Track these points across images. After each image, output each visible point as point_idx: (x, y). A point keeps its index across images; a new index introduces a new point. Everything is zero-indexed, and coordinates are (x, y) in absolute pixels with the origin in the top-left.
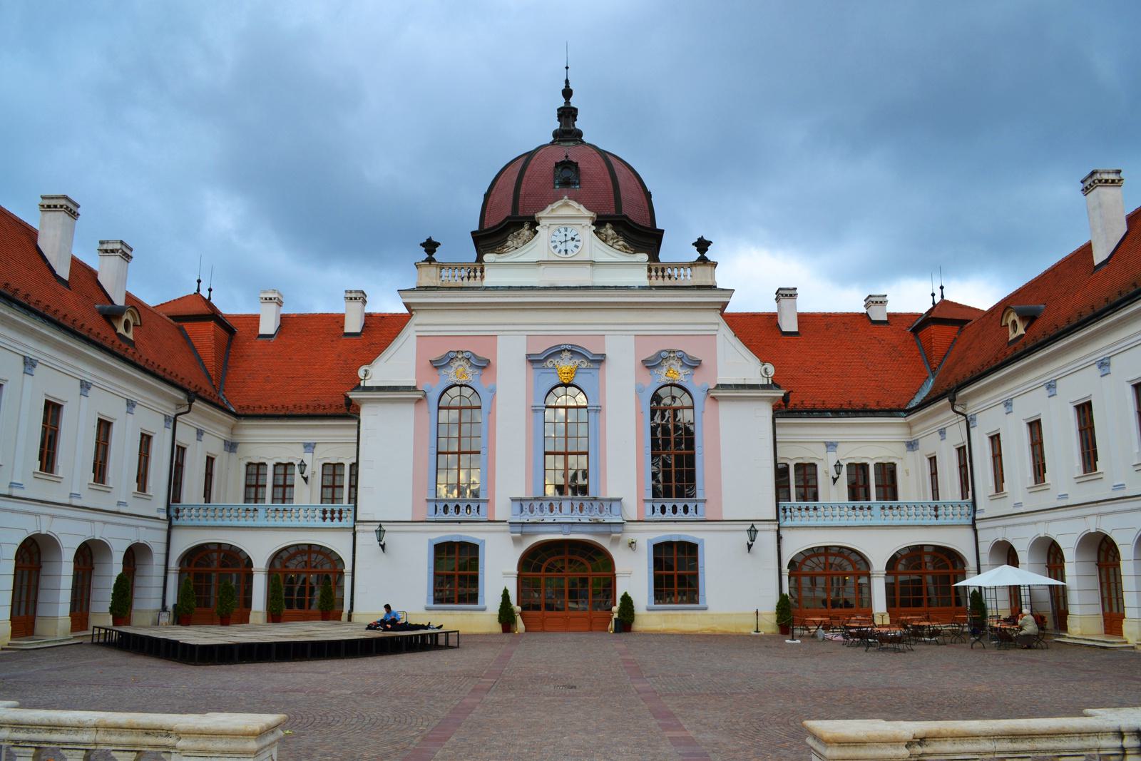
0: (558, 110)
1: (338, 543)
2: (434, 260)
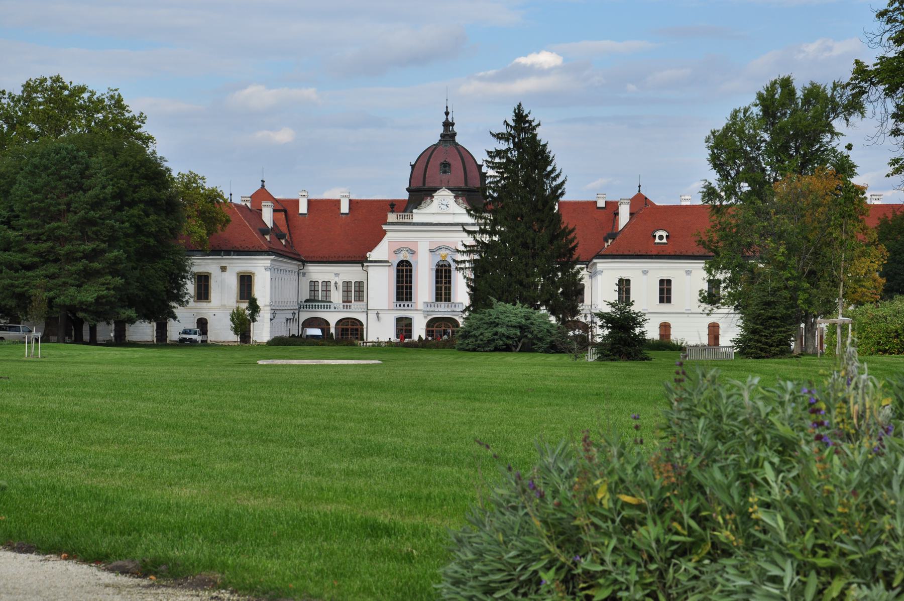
1: (361, 317)
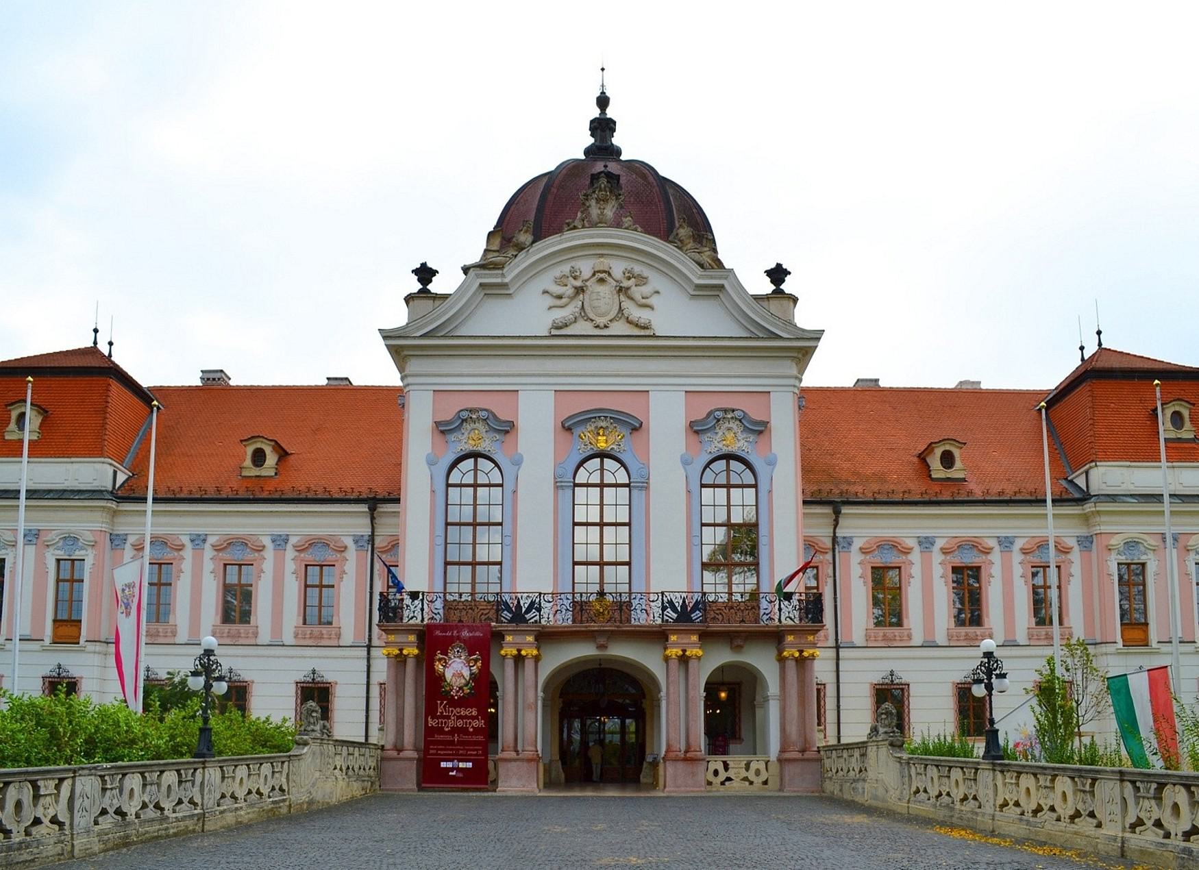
0: (592, 122)
2: (429, 291)
